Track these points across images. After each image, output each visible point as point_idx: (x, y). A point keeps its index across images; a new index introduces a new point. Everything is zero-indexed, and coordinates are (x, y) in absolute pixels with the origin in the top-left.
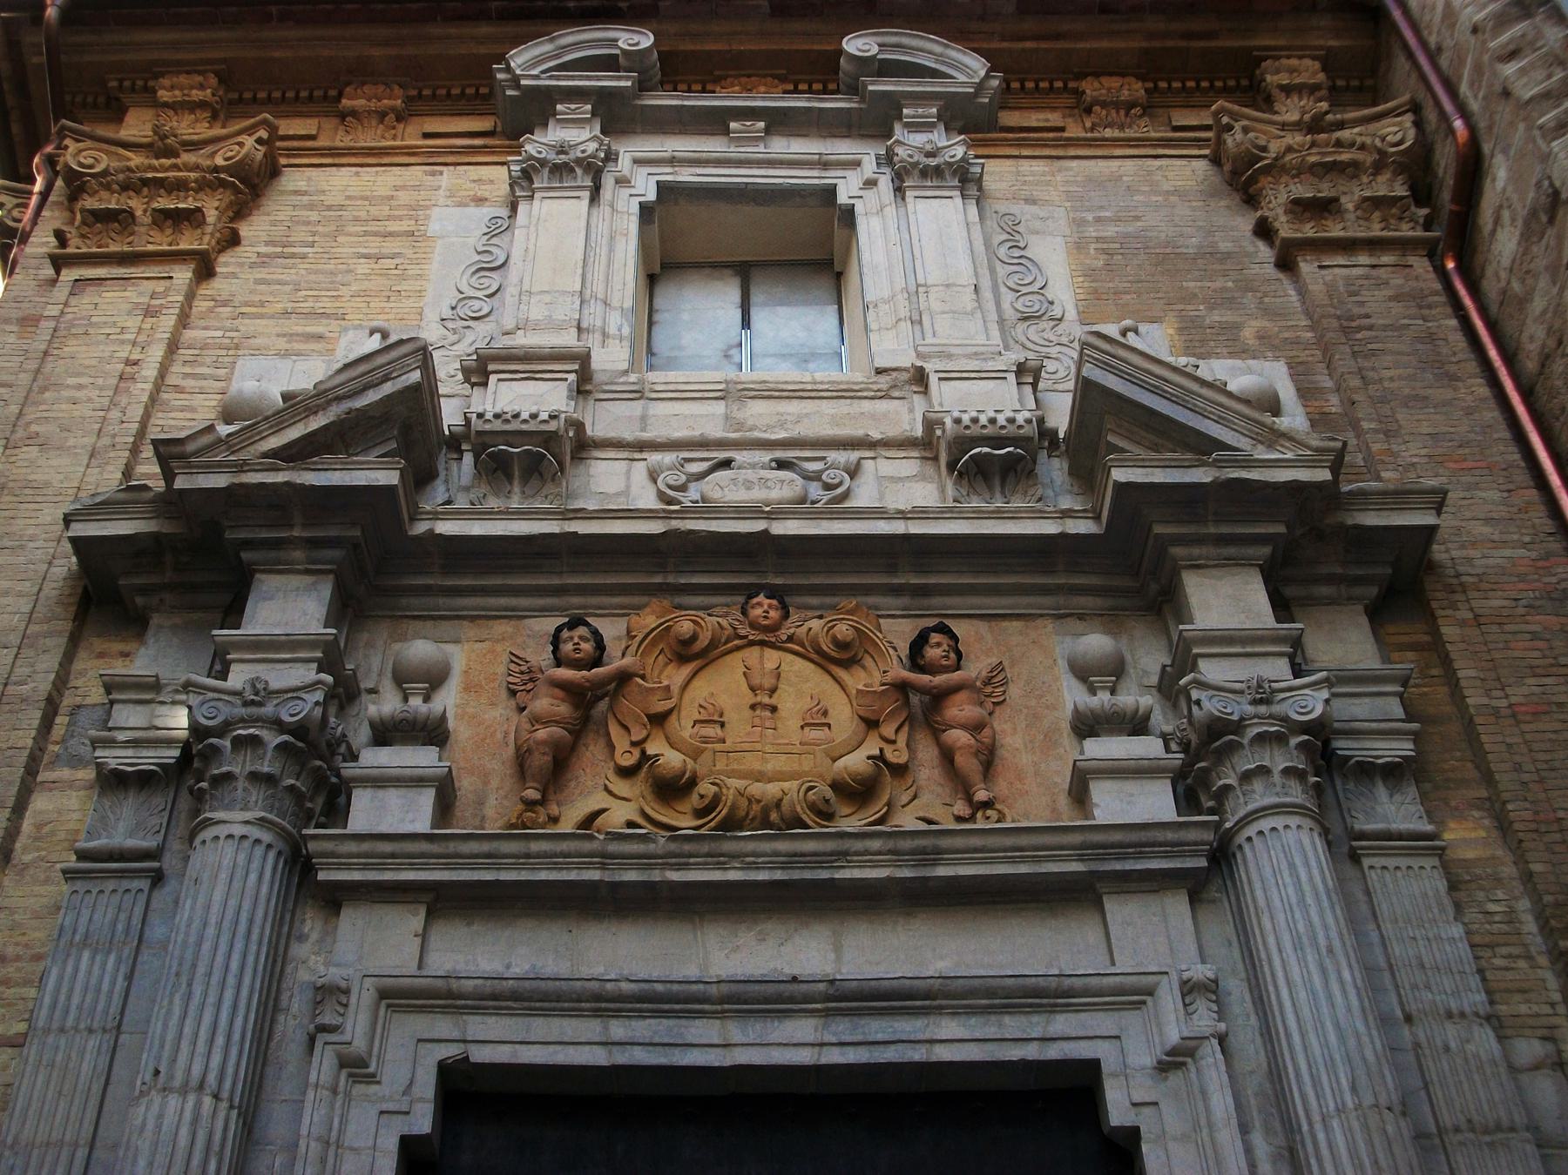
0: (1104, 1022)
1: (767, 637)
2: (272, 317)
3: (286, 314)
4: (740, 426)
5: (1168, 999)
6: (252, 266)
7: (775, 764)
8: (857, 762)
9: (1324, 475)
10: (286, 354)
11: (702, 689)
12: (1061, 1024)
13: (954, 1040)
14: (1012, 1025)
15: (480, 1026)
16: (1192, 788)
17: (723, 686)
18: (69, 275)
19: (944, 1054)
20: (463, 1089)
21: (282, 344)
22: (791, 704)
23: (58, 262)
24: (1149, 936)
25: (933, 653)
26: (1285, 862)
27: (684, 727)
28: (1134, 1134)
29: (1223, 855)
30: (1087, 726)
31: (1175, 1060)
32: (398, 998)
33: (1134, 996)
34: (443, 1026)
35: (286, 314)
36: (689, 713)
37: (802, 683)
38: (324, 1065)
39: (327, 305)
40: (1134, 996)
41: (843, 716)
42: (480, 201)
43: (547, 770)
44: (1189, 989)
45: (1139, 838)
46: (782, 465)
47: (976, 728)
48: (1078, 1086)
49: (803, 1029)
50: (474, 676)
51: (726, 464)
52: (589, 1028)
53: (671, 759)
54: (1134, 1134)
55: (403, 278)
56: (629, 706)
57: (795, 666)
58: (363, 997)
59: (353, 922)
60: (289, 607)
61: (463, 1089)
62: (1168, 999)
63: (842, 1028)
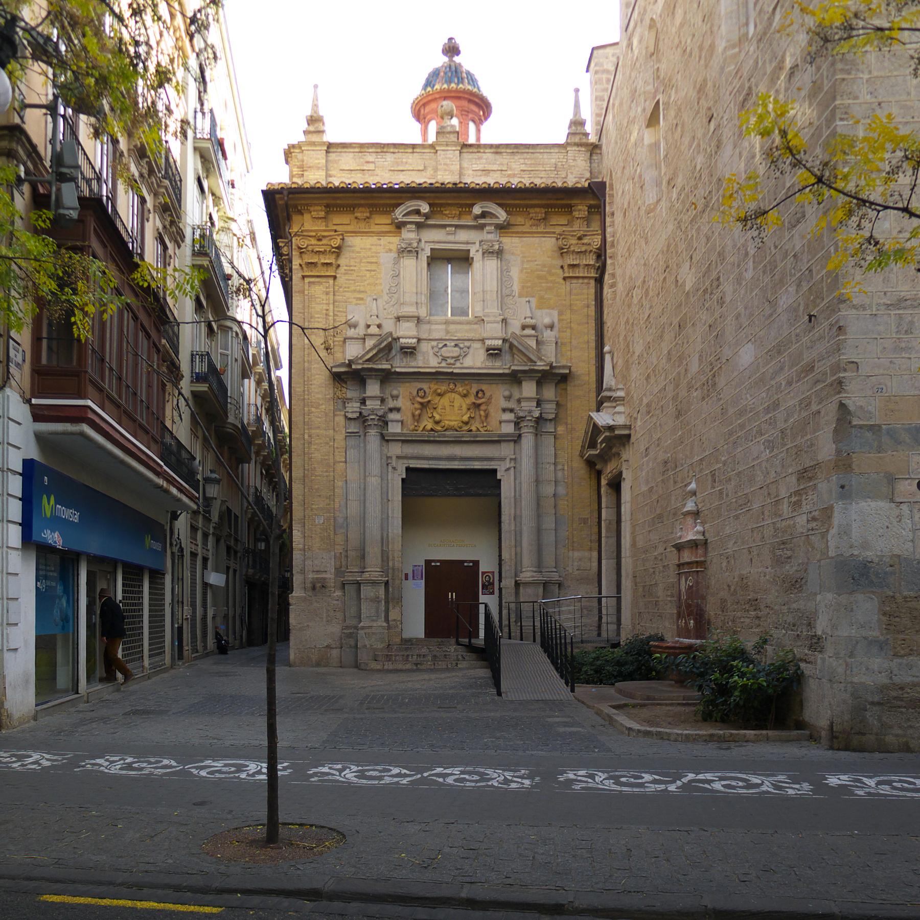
0: (499, 463)
1: (453, 391)
2: (351, 292)
3: (355, 291)
4: (448, 332)
5: (508, 461)
6: (345, 274)
7: (453, 418)
8: (465, 418)
9: (548, 368)
10: (357, 304)
11: (442, 401)
12: (493, 463)
13: (477, 465)
14: (485, 463)
15: (411, 461)
16: (517, 424)
17: (445, 401)
18: (307, 280)
19: (476, 467)
20: (408, 469)
21: (355, 301)
22: (457, 404)
23: (304, 277)
24: (506, 450)
25: (480, 395)
26: (528, 441)
27: (439, 410)
28: (500, 480)
29: (520, 436)
30: (504, 410)
31: (508, 469)
32: (398, 457)
33: (503, 459)
34: (405, 461)
35: (355, 291)
36: (440, 407)
37: (458, 401)
38: (390, 468)
39: (362, 289)
40: (503, 459)
41: (464, 407)
42: (391, 250)
43: (417, 419)
44: (511, 459)
45: (507, 435)
46: (456, 345)
47: (485, 411)
48: (495, 471)
49: (456, 463)
50: (403, 397)
51: (445, 345)
52: (426, 462)
53: (437, 417)
54: (500, 480)
55: (377, 279)
56: (430, 406)
57: (457, 396)
58: (394, 458)
59: (391, 444)
60: (373, 389)
61: (408, 469)
62: (508, 461)
63: (462, 463)
